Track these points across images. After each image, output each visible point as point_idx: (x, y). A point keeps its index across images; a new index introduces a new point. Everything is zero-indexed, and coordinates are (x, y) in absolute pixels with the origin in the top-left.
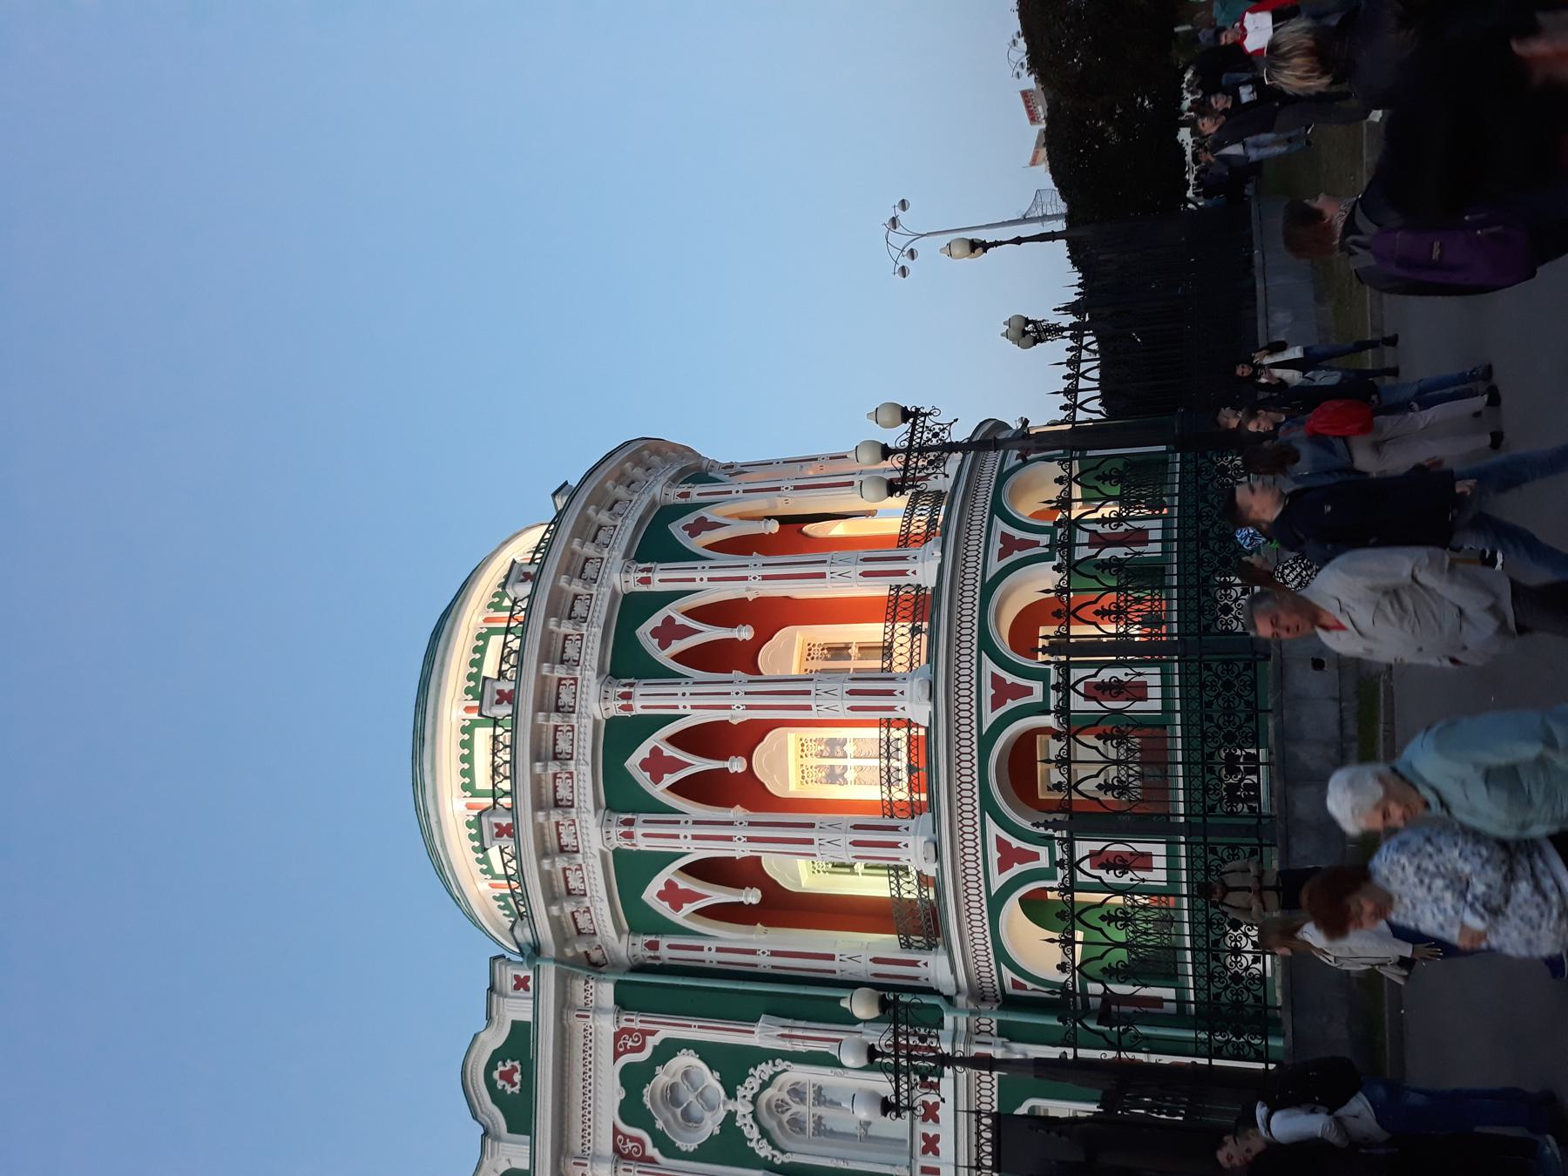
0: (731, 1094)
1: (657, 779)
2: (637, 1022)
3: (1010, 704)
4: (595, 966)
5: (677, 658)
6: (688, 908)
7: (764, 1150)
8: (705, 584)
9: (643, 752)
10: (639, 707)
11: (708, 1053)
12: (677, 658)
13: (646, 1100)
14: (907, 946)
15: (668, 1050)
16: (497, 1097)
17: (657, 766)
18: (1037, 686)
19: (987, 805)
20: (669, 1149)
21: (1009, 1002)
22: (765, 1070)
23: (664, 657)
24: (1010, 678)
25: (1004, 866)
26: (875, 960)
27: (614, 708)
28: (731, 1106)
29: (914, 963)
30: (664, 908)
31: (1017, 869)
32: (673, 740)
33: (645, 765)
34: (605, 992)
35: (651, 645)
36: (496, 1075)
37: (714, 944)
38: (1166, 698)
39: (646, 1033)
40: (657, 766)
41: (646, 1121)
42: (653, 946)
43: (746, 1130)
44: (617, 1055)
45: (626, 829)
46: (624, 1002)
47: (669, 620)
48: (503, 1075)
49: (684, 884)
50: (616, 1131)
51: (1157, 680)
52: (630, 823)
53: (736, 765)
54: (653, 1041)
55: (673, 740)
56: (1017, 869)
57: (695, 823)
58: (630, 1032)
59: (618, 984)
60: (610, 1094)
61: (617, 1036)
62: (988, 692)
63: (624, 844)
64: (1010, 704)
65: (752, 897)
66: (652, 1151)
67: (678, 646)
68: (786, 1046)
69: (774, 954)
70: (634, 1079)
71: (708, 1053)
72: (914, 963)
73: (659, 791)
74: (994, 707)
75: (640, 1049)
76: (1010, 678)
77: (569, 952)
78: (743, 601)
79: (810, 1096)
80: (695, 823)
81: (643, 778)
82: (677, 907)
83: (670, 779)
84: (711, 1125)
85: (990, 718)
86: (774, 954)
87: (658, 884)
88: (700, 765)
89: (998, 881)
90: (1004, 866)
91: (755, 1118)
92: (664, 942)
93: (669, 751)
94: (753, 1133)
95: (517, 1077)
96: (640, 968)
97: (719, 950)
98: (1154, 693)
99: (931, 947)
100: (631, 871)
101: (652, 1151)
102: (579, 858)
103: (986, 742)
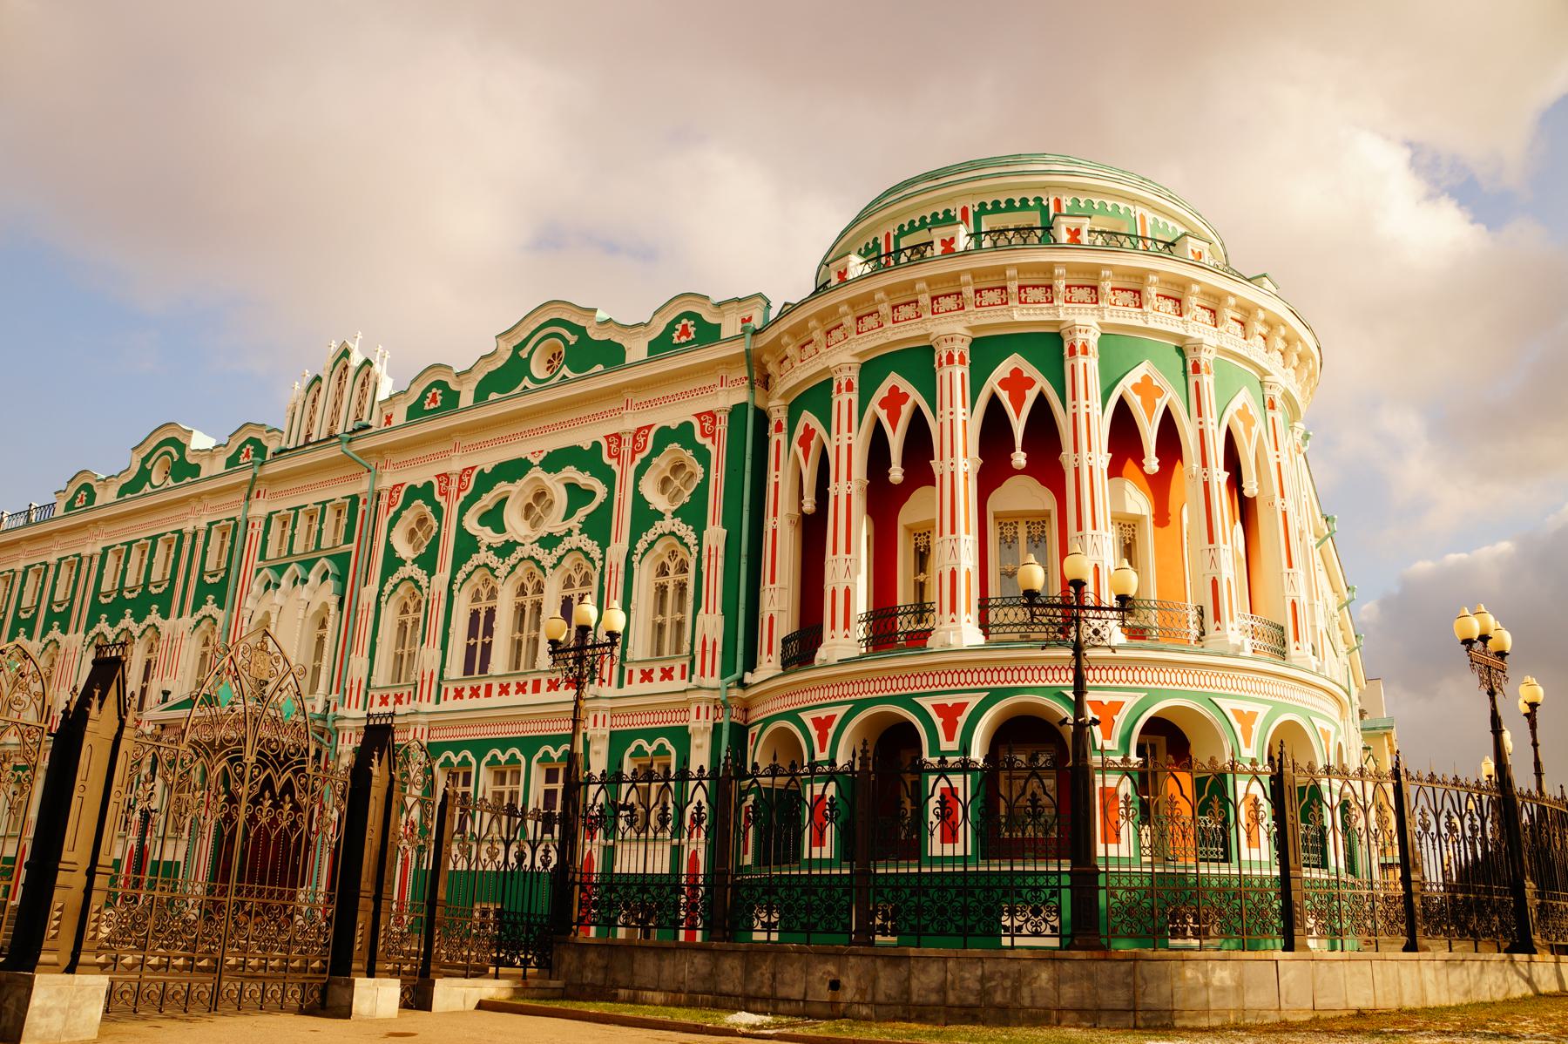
0: (675, 514)
1: (883, 404)
2: (722, 427)
3: (938, 721)
4: (762, 380)
5: (994, 401)
6: (800, 451)
7: (641, 546)
8: (1070, 410)
9: (905, 386)
11: (702, 489)
12: (994, 401)
13: (670, 446)
14: (785, 641)
15: (703, 456)
16: (670, 327)
18: (954, 745)
20: (640, 473)
21: (740, 734)
22: (691, 539)
23: (993, 382)
24: (962, 720)
25: (816, 721)
26: (771, 619)
28: (669, 515)
29: (770, 651)
30: (799, 431)
31: (814, 733)
32: (917, 411)
33: (894, 389)
34: (740, 396)
35: (1003, 370)
36: (684, 321)
37: (780, 480)
38: (942, 860)
39: (713, 435)
41: (657, 450)
42: (779, 428)
43: (652, 530)
44: (698, 416)
45: (843, 386)
46: (737, 412)
47: (1030, 383)
48: (685, 326)
49: (813, 443)
50: (649, 427)
51: (960, 852)
52: (849, 387)
53: (896, 474)
54: (707, 442)
55: (917, 411)
56: (814, 733)
57: (849, 446)
58: (714, 423)
59: (746, 404)
60: (672, 416)
61: (710, 413)
62: (950, 701)
64: (938, 721)
65: (809, 506)
66: (639, 458)
67: (1004, 396)
68: (705, 553)
69: (774, 531)
70: (683, 434)
71: (702, 489)
72: (770, 651)
73: (874, 405)
74: (934, 706)
75: (704, 435)
76: (962, 720)
77: (766, 358)
78: (1058, 448)
79: (681, 577)
80: (849, 446)
81: (882, 392)
82: (800, 444)
84: (658, 502)
85: (927, 704)
86: (774, 531)
89: (807, 718)
90: (816, 721)
91: (661, 535)
92: (783, 437)
93: (906, 411)
94: (650, 535)
95: (684, 339)
96: (762, 418)
97: (777, 484)
98: (948, 850)
99: (785, 664)
100: (817, 397)
101: (639, 458)
102: (823, 350)
103: (907, 701)
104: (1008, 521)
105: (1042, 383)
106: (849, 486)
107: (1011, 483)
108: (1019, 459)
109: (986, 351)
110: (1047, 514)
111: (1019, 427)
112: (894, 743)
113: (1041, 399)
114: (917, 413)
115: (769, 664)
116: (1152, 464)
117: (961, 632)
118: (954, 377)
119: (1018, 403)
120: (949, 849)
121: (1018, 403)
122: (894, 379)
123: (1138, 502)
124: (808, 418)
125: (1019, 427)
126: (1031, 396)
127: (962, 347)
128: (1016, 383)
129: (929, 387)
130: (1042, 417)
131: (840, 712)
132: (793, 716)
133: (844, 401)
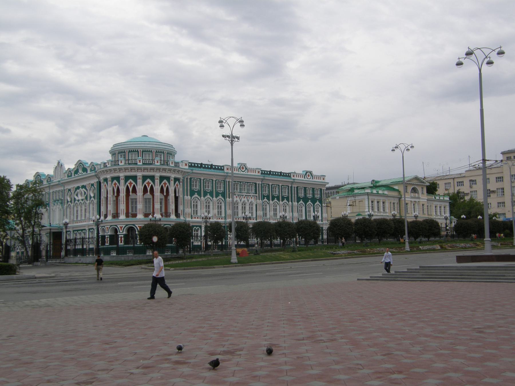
5: (145, 185)
9: (132, 182)
10: (138, 181)
12: (145, 185)
17: (131, 183)
19: (127, 225)
23: (145, 183)
27: (138, 177)
30: (114, 183)
32: (134, 185)
35: (147, 181)
40: (131, 183)
53: (131, 193)
55: (134, 185)
63: (121, 178)
65: (116, 194)
67: (147, 185)
73: (127, 183)
78: (153, 192)
81: (129, 182)
83: (129, 185)
85: (137, 226)
87: (117, 182)
88: (131, 189)
89: (119, 226)
104: (146, 199)
105: (152, 183)
106: (123, 194)
107: (146, 194)
108: (149, 193)
109: (145, 178)
110: (150, 199)
111: (149, 189)
112: (131, 229)
113: (152, 186)
114: (134, 186)
115: (109, 218)
116: (165, 194)
117: (140, 216)
118: (140, 181)
119: (149, 186)
120: (138, 244)
121: (149, 186)
122: (131, 180)
123: (163, 197)
124: (115, 181)
125: (149, 189)
126: (150, 185)
127: (141, 177)
128: (149, 183)
129: (136, 182)
130: (152, 188)
131: (124, 226)
132: (116, 225)
133: (122, 182)
